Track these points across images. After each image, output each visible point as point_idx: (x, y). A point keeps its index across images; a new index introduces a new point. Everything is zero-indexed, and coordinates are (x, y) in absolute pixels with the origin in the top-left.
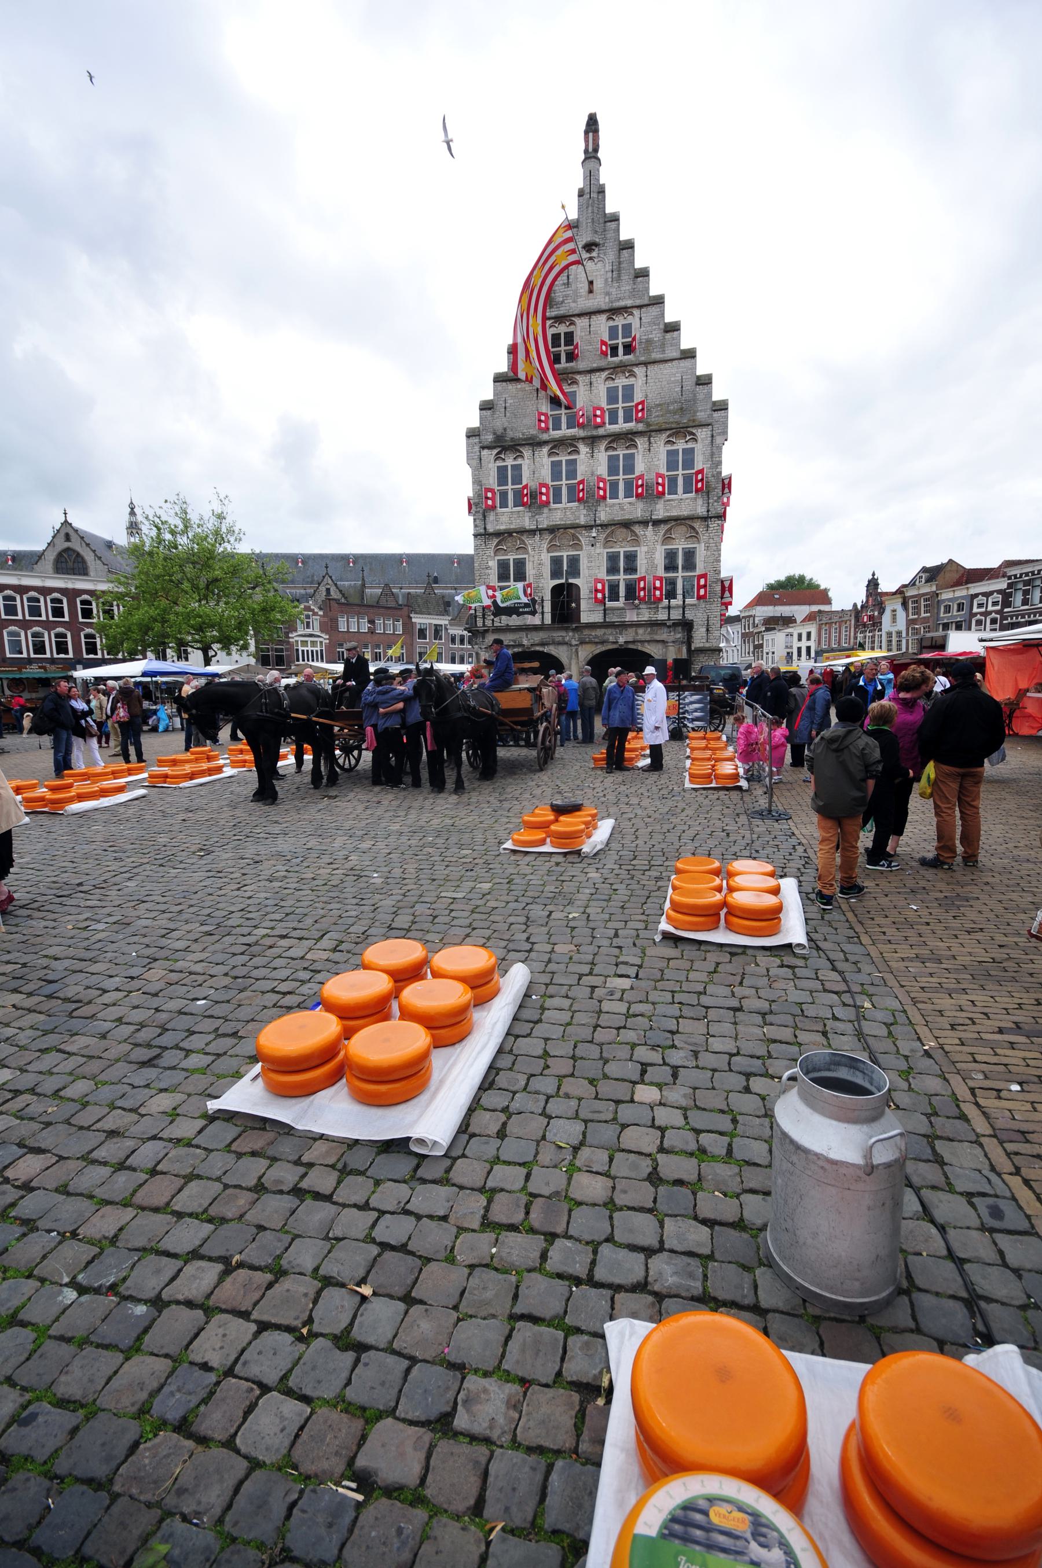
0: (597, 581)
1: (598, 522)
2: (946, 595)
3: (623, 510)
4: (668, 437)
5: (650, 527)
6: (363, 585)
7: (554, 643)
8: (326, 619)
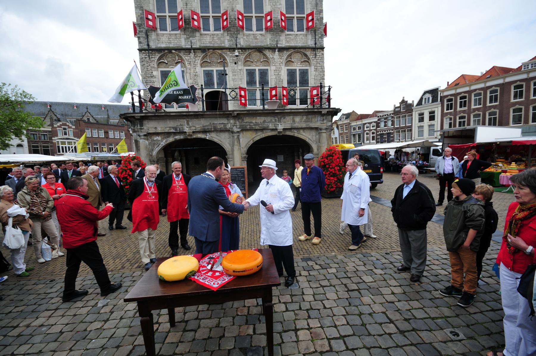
0: (241, 89)
1: (239, 46)
2: (354, 124)
3: (256, 39)
5: (277, 53)
6: (108, 117)
7: (216, 130)
8: (77, 131)
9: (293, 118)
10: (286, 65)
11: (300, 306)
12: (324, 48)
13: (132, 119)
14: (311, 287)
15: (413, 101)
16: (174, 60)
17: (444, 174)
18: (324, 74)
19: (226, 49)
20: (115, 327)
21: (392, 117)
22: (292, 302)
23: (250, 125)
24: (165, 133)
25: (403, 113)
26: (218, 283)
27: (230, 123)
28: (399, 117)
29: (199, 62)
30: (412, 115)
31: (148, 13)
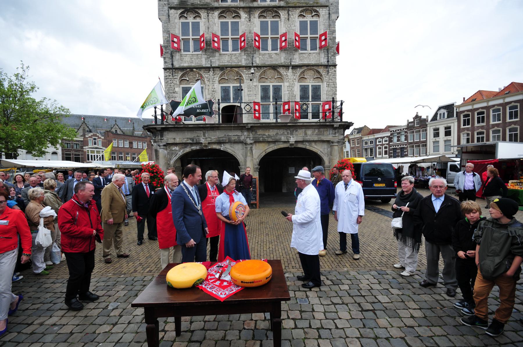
0: (255, 103)
1: (255, 64)
2: (365, 138)
3: (271, 58)
4: (301, 11)
5: (290, 70)
6: (134, 129)
7: (230, 142)
8: (105, 141)
9: (305, 131)
10: (299, 82)
11: (310, 323)
12: (336, 65)
13: (154, 130)
14: (322, 304)
15: (427, 117)
16: (194, 78)
17: (464, 190)
18: (336, 90)
19: (243, 67)
20: (122, 332)
21: (406, 132)
22: (301, 319)
23: (263, 137)
24: (183, 143)
25: (417, 128)
26: (226, 294)
27: (244, 135)
28: (413, 132)
29: (217, 79)
30: (426, 130)
31: (174, 36)
